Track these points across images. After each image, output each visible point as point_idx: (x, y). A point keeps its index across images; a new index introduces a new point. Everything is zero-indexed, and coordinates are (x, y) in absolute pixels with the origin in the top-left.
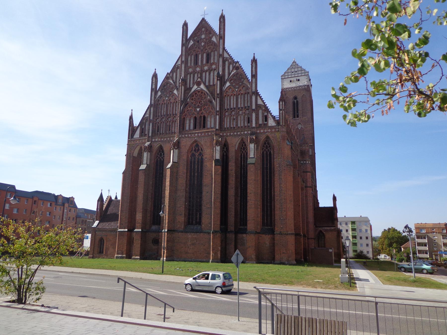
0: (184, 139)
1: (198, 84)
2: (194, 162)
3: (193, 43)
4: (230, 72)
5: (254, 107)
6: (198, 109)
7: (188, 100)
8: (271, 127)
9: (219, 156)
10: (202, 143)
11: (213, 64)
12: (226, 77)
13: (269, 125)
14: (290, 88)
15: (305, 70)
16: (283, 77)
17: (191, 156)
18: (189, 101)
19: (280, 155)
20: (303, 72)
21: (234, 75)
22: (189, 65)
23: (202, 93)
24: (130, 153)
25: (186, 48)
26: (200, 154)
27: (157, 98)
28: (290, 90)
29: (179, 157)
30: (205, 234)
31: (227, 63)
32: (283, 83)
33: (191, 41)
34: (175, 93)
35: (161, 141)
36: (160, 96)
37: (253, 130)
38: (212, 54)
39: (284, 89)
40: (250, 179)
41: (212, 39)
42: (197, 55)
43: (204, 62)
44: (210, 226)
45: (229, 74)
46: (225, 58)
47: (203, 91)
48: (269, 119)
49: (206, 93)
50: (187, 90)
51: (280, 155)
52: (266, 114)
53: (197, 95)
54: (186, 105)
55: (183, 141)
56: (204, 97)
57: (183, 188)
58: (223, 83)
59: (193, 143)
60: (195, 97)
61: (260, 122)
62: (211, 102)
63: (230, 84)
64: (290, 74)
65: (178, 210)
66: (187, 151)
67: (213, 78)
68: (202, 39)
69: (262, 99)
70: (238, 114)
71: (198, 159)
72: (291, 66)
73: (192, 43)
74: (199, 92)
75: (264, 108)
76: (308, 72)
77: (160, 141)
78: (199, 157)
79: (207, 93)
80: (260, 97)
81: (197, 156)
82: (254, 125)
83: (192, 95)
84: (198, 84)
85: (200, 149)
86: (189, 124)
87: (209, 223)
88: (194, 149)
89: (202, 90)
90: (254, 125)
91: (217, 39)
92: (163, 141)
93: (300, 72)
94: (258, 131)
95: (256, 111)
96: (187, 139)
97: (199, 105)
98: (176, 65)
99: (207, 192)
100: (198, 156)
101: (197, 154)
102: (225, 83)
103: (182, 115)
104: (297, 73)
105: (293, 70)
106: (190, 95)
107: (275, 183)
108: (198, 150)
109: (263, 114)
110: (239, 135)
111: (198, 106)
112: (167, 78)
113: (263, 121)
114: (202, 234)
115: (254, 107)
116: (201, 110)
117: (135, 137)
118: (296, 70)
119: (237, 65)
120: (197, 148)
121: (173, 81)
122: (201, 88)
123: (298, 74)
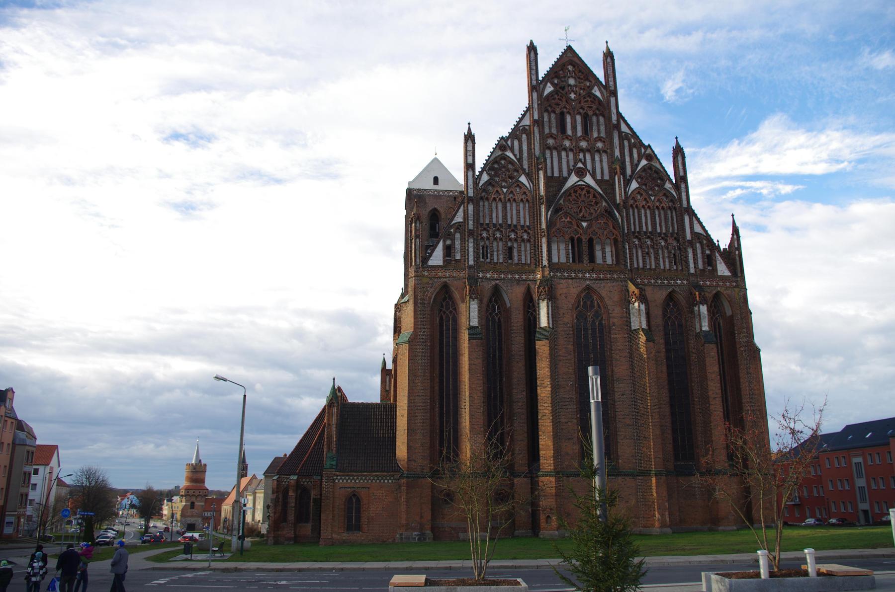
0: (562, 281)
1: (581, 173)
2: (586, 330)
3: (552, 89)
4: (636, 161)
5: (689, 237)
6: (584, 224)
7: (561, 201)
8: (724, 278)
9: (645, 322)
10: (603, 293)
11: (599, 139)
12: (629, 171)
13: (720, 273)
17: (576, 317)
18: (563, 203)
19: (744, 330)
21: (644, 169)
22: (547, 131)
23: (588, 192)
25: (540, 96)
26: (597, 315)
27: (481, 184)
29: (554, 316)
30: (627, 478)
31: (626, 143)
33: (549, 84)
34: (520, 182)
35: (501, 280)
37: (691, 279)
38: (594, 118)
40: (710, 371)
41: (593, 91)
43: (579, 133)
44: (634, 461)
45: (634, 166)
46: (623, 134)
47: (591, 190)
48: (718, 262)
49: (597, 195)
51: (744, 330)
52: (708, 252)
53: (578, 195)
54: (556, 211)
55: (561, 286)
56: (594, 201)
57: (570, 383)
59: (582, 292)
62: (610, 214)
63: (638, 186)
65: (562, 430)
66: (570, 306)
67: (602, 165)
68: (570, 85)
71: (594, 322)
73: (549, 89)
74: (582, 189)
77: (497, 279)
78: (594, 320)
80: (698, 220)
81: (590, 319)
82: (692, 271)
84: (581, 173)
85: (596, 305)
87: (632, 456)
88: (582, 303)
89: (588, 186)
90: (692, 271)
92: (504, 280)
94: (481, 275)
95: (691, 244)
96: (570, 281)
97: (586, 215)
98: (521, 125)
99: (623, 394)
100: (592, 318)
101: (590, 314)
102: (627, 183)
103: (551, 231)
106: (564, 192)
107: (742, 380)
108: (592, 306)
109: (703, 252)
110: (669, 285)
111: (583, 216)
112: (502, 145)
113: (704, 264)
114: (620, 478)
115: (689, 237)
116: (589, 227)
117: (431, 262)
119: (649, 151)
120: (589, 303)
121: (515, 155)
122: (584, 182)
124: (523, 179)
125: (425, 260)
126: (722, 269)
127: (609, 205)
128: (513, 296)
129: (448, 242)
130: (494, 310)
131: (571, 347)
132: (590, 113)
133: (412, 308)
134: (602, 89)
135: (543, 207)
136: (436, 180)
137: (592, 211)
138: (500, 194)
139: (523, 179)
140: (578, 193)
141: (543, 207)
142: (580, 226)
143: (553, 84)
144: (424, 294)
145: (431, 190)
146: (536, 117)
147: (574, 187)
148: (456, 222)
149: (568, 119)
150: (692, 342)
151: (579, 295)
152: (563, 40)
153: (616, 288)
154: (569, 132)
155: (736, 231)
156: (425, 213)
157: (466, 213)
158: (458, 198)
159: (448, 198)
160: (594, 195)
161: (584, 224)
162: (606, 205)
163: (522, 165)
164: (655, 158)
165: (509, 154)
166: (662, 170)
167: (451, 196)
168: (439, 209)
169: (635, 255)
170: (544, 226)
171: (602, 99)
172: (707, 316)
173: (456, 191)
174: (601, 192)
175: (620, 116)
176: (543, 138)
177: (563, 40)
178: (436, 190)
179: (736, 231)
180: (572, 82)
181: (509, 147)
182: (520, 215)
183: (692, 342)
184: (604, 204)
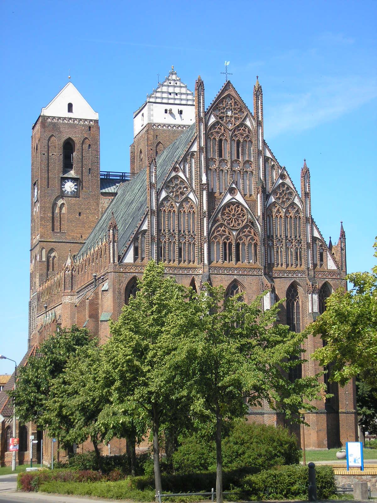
6: (234, 233)
8: (331, 272)
10: (245, 284)
14: (164, 125)
24: (119, 289)
28: (164, 130)
30: (258, 416)
32: (152, 112)
33: (212, 116)
34: (189, 198)
36: (166, 199)
39: (154, 125)
42: (220, 141)
43: (235, 157)
56: (242, 214)
58: (266, 197)
60: (227, 211)
62: (252, 223)
64: (165, 95)
69: (318, 229)
73: (213, 120)
79: (246, 209)
80: (316, 226)
86: (218, 251)
91: (252, 123)
93: (184, 97)
104: (178, 97)
105: (171, 90)
111: (233, 226)
116: (239, 234)
118: (177, 90)
121: (185, 176)
123: (181, 99)
125: (121, 259)
127: (252, 217)
132: (241, 140)
133: (112, 295)
134: (252, 119)
135: (205, 219)
137: (240, 222)
138: (174, 207)
139: (191, 196)
140: (231, 207)
141: (205, 219)
142: (231, 234)
143: (216, 116)
144: (120, 285)
145: (65, 118)
146: (202, 144)
147: (228, 204)
148: (142, 229)
150: (306, 319)
152: (224, 73)
153: (254, 281)
155: (343, 235)
156: (58, 142)
157: (151, 223)
158: (93, 127)
159: (83, 128)
160: (242, 209)
162: (251, 217)
163: (191, 184)
164: (288, 177)
165: (181, 174)
166: (292, 187)
167: (86, 125)
168: (74, 139)
169: (269, 254)
170: (205, 234)
171: (251, 128)
172: (317, 301)
173: (91, 120)
174: (248, 208)
176: (207, 160)
177: (224, 73)
178: (70, 119)
179: (343, 235)
180: (229, 113)
181: (181, 169)
183: (306, 319)
184: (249, 216)
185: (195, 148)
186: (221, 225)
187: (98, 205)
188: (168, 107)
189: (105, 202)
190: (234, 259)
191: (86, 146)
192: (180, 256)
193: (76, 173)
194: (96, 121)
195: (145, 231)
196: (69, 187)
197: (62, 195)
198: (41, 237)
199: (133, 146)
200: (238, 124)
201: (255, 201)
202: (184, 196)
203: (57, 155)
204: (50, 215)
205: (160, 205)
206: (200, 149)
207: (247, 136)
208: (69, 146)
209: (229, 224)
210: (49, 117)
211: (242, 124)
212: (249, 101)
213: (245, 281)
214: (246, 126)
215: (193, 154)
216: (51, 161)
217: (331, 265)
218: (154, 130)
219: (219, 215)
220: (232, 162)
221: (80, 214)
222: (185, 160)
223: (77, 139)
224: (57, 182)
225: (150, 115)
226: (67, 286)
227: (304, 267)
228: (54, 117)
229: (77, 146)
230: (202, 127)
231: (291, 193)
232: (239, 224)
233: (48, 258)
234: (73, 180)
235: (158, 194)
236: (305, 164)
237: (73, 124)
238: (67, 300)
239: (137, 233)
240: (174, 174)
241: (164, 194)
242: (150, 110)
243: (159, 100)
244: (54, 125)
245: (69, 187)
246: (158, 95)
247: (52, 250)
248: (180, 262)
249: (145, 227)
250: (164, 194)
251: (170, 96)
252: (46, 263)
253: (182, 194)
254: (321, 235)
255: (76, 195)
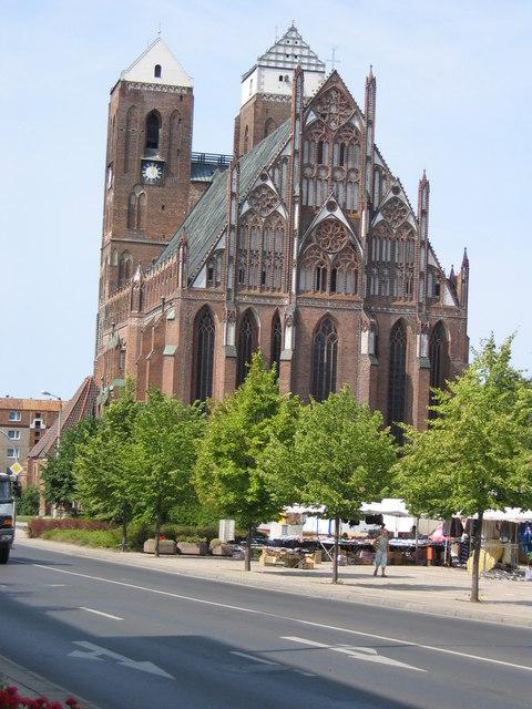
1: (331, 207)
5: (423, 268)
6: (330, 256)
8: (449, 309)
12: (376, 205)
14: (278, 96)
15: (316, 58)
16: (264, 64)
20: (314, 61)
21: (390, 202)
22: (306, 161)
25: (304, 123)
31: (377, 175)
42: (321, 143)
43: (335, 164)
50: (307, 213)
58: (372, 215)
61: (430, 295)
62: (354, 246)
64: (281, 58)
67: (354, 198)
70: (393, 276)
72: (286, 37)
73: (312, 118)
75: (436, 274)
76: (324, 66)
83: (320, 226)
84: (331, 207)
86: (309, 280)
89: (337, 222)
91: (361, 123)
104: (296, 60)
105: (289, 51)
118: (297, 52)
124: (281, 210)
125: (190, 282)
126: (448, 300)
128: (263, 321)
129: (211, 266)
130: (246, 328)
131: (309, 366)
132: (347, 143)
136: (158, 70)
139: (281, 210)
143: (316, 113)
147: (326, 222)
149: (327, 150)
151: (320, 321)
154: (326, 162)
155: (466, 264)
156: (141, 115)
161: (330, 256)
165: (269, 183)
170: (295, 258)
173: (184, 88)
174: (347, 225)
175: (375, 148)
176: (303, 167)
178: (157, 85)
179: (466, 264)
180: (334, 110)
182: (276, 243)
185: (288, 152)
186: (315, 247)
187: (187, 196)
188: (284, 74)
189: (195, 194)
190: (328, 288)
191: (176, 120)
192: (263, 282)
193: (162, 155)
194: (190, 89)
195: (222, 251)
196: (152, 173)
197: (142, 182)
198: (113, 235)
199: (238, 119)
200: (343, 123)
201: (359, 220)
202: (271, 211)
203: (138, 132)
204: (125, 207)
205: (242, 219)
206: (295, 152)
207: (355, 139)
208: (153, 119)
209: (324, 246)
210: (131, 83)
211: (349, 124)
212: (359, 98)
213: (340, 316)
214: (353, 127)
215: (285, 160)
216: (131, 139)
217: (448, 300)
218: (264, 102)
219: (313, 234)
220: (334, 170)
221: (163, 207)
222: (275, 165)
223: (164, 111)
224: (135, 166)
225: (260, 83)
226: (134, 306)
227: (414, 303)
228: (137, 83)
229: (164, 121)
230: (298, 124)
231: (405, 211)
232: (337, 247)
233: (120, 261)
234: (159, 164)
235: (240, 206)
236: (425, 176)
237: (160, 92)
238: (133, 322)
239: (213, 252)
240: (260, 182)
241: (246, 207)
242: (260, 76)
243: (273, 64)
244: (136, 93)
245: (152, 173)
246: (273, 57)
247: (126, 251)
248: (262, 289)
249: (221, 245)
250: (246, 207)
251: (287, 60)
252: (117, 269)
253: (270, 206)
254: (438, 264)
255: (159, 183)
